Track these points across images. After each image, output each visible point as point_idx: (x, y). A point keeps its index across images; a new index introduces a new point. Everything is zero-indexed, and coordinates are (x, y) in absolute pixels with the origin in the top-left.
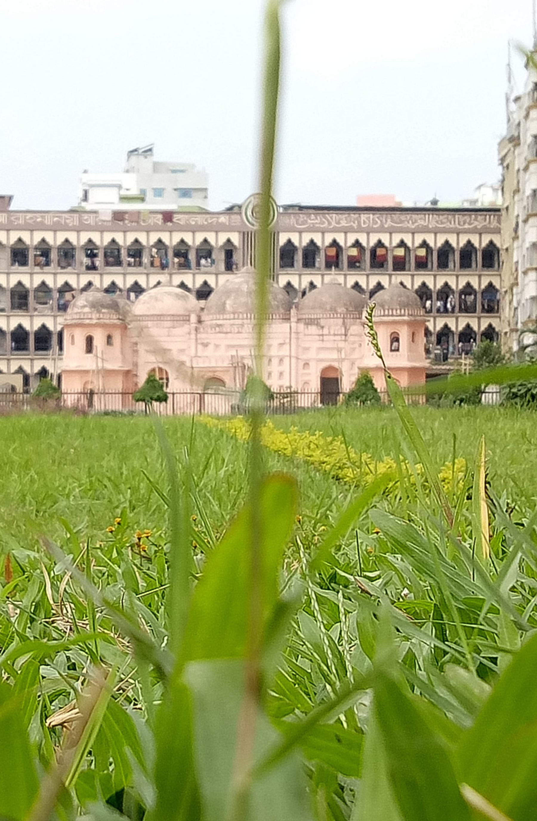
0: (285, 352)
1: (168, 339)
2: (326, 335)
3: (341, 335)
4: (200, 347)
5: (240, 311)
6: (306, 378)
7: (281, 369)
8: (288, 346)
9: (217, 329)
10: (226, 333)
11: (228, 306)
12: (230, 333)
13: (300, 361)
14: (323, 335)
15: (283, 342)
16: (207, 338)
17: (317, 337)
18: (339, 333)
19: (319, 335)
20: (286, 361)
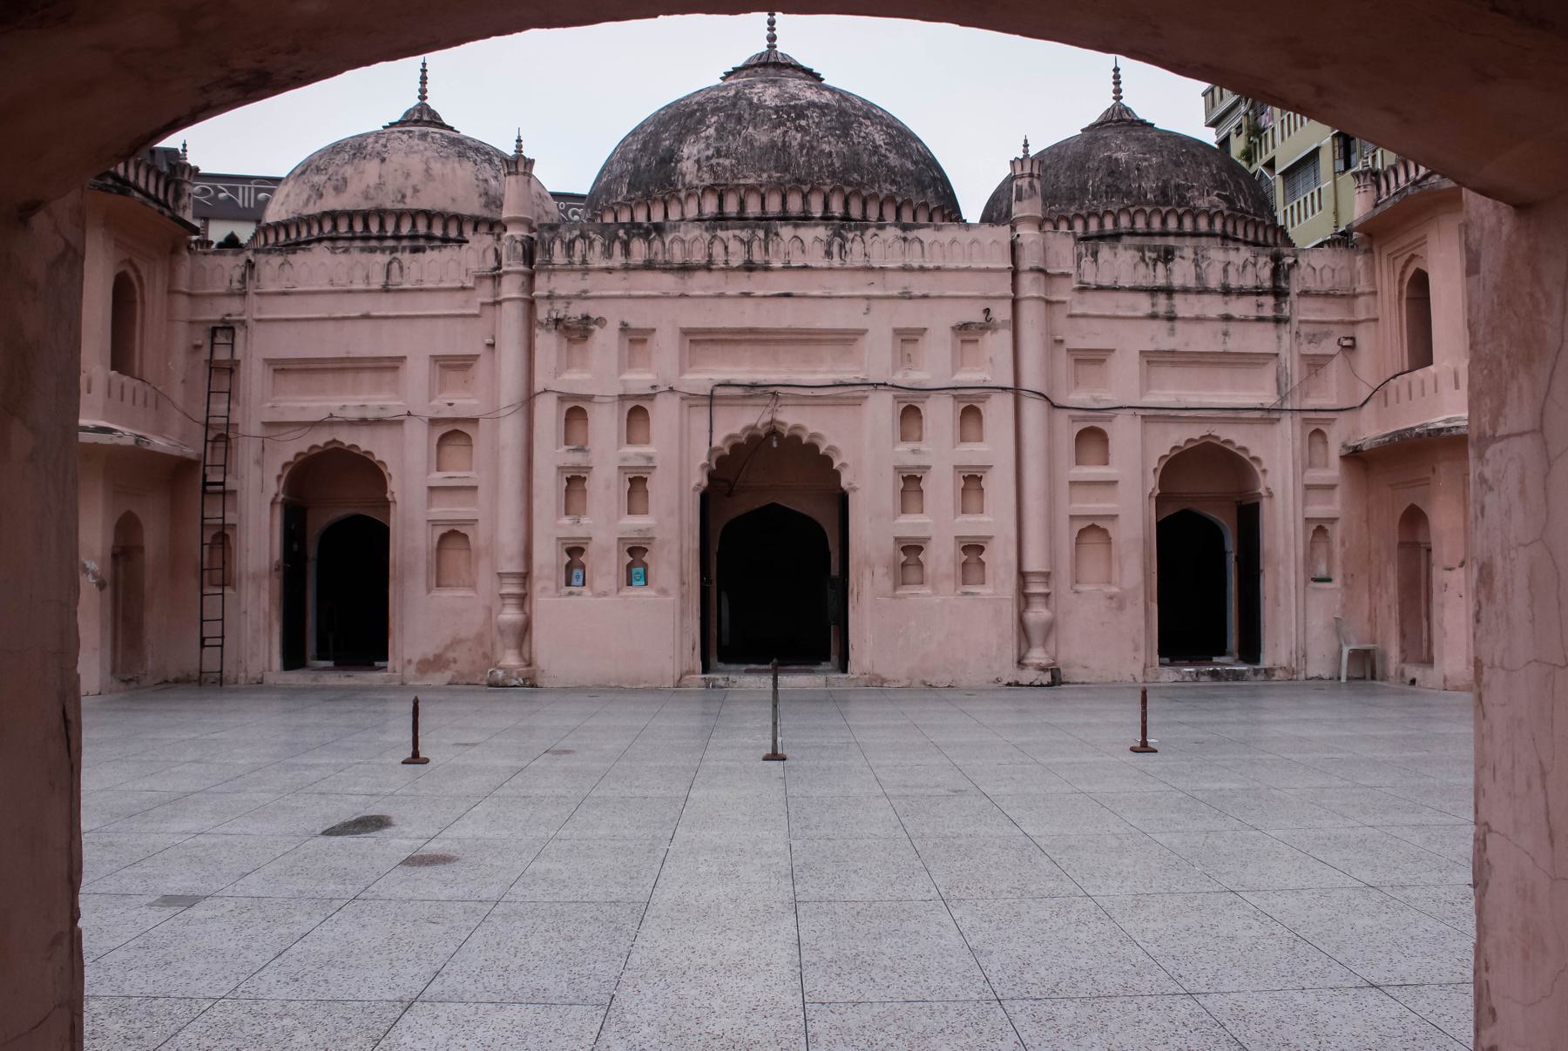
0: (989, 364)
1: (386, 306)
2: (1186, 290)
3: (1258, 292)
4: (546, 342)
5: (751, 181)
6: (1094, 505)
7: (972, 453)
8: (1005, 335)
9: (639, 249)
10: (686, 269)
11: (688, 166)
12: (708, 267)
13: (1063, 416)
14: (1169, 291)
15: (979, 317)
16: (583, 296)
17: (1143, 304)
18: (1249, 282)
19: (1153, 291)
20: (997, 411)
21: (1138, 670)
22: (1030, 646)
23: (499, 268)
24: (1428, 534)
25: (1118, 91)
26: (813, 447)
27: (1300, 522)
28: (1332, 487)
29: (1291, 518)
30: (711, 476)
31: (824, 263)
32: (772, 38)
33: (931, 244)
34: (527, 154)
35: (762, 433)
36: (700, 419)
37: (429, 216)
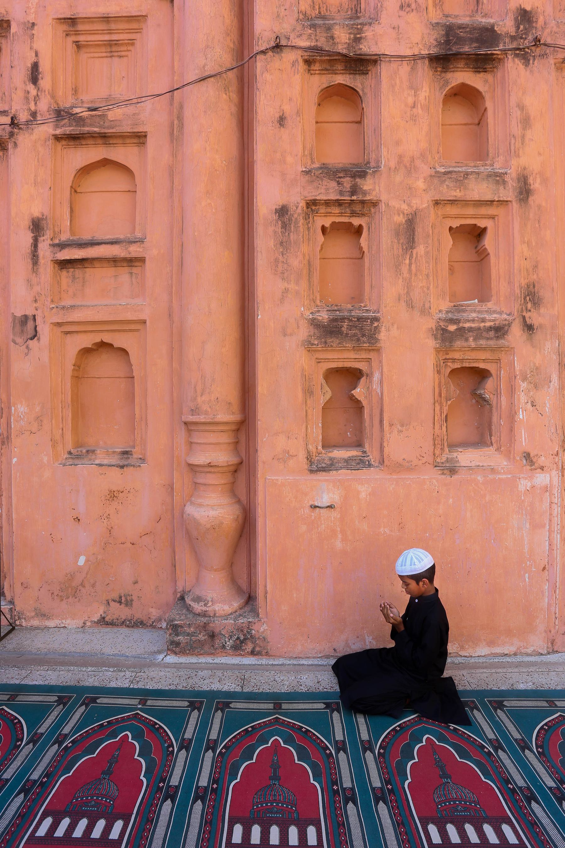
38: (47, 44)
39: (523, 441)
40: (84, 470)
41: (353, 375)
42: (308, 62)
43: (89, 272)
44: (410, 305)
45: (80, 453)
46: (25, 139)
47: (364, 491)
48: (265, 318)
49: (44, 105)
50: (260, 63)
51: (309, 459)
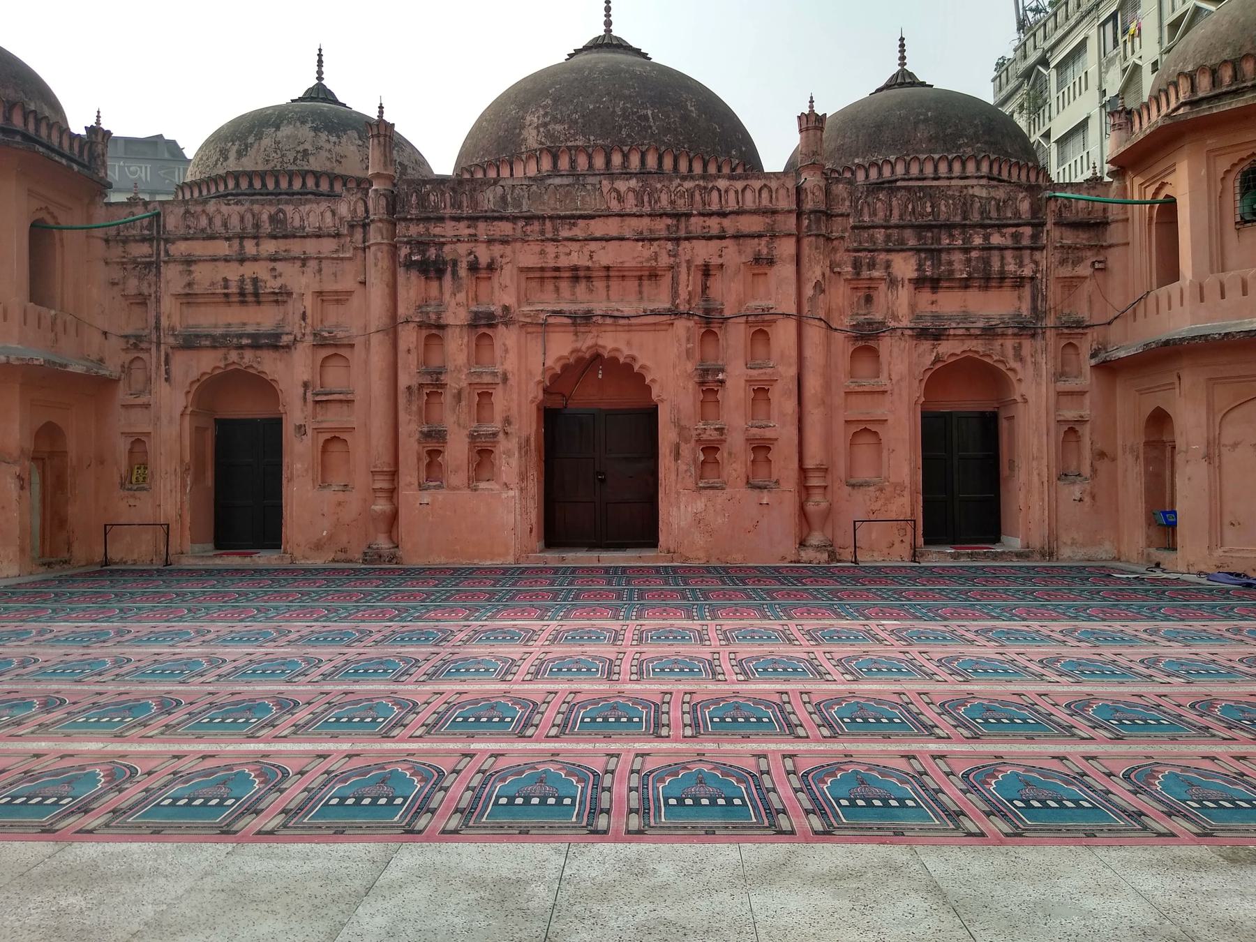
2: (949, 227)
13: (839, 337)
20: (784, 335)
21: (905, 550)
22: (810, 529)
23: (367, 217)
24: (1173, 433)
25: (903, 58)
26: (628, 367)
27: (1053, 425)
28: (1083, 393)
29: (1044, 420)
30: (546, 391)
31: (635, 210)
32: (608, 24)
33: (726, 191)
34: (387, 117)
35: (587, 356)
36: (535, 346)
37: (317, 176)
38: (308, 301)
39: (504, 478)
40: (327, 493)
41: (440, 452)
42: (420, 326)
43: (329, 405)
44: (459, 425)
45: (324, 484)
46: (299, 346)
47: (440, 498)
48: (402, 430)
49: (308, 330)
50: (400, 328)
51: (420, 485)
